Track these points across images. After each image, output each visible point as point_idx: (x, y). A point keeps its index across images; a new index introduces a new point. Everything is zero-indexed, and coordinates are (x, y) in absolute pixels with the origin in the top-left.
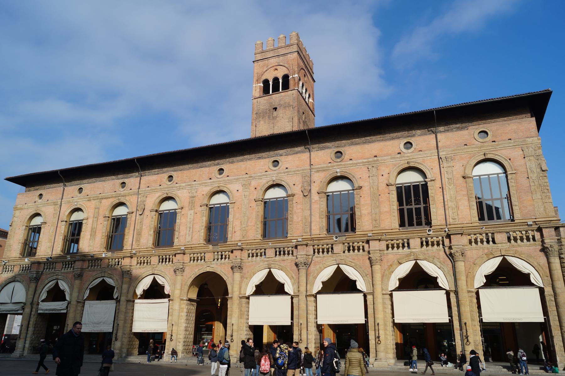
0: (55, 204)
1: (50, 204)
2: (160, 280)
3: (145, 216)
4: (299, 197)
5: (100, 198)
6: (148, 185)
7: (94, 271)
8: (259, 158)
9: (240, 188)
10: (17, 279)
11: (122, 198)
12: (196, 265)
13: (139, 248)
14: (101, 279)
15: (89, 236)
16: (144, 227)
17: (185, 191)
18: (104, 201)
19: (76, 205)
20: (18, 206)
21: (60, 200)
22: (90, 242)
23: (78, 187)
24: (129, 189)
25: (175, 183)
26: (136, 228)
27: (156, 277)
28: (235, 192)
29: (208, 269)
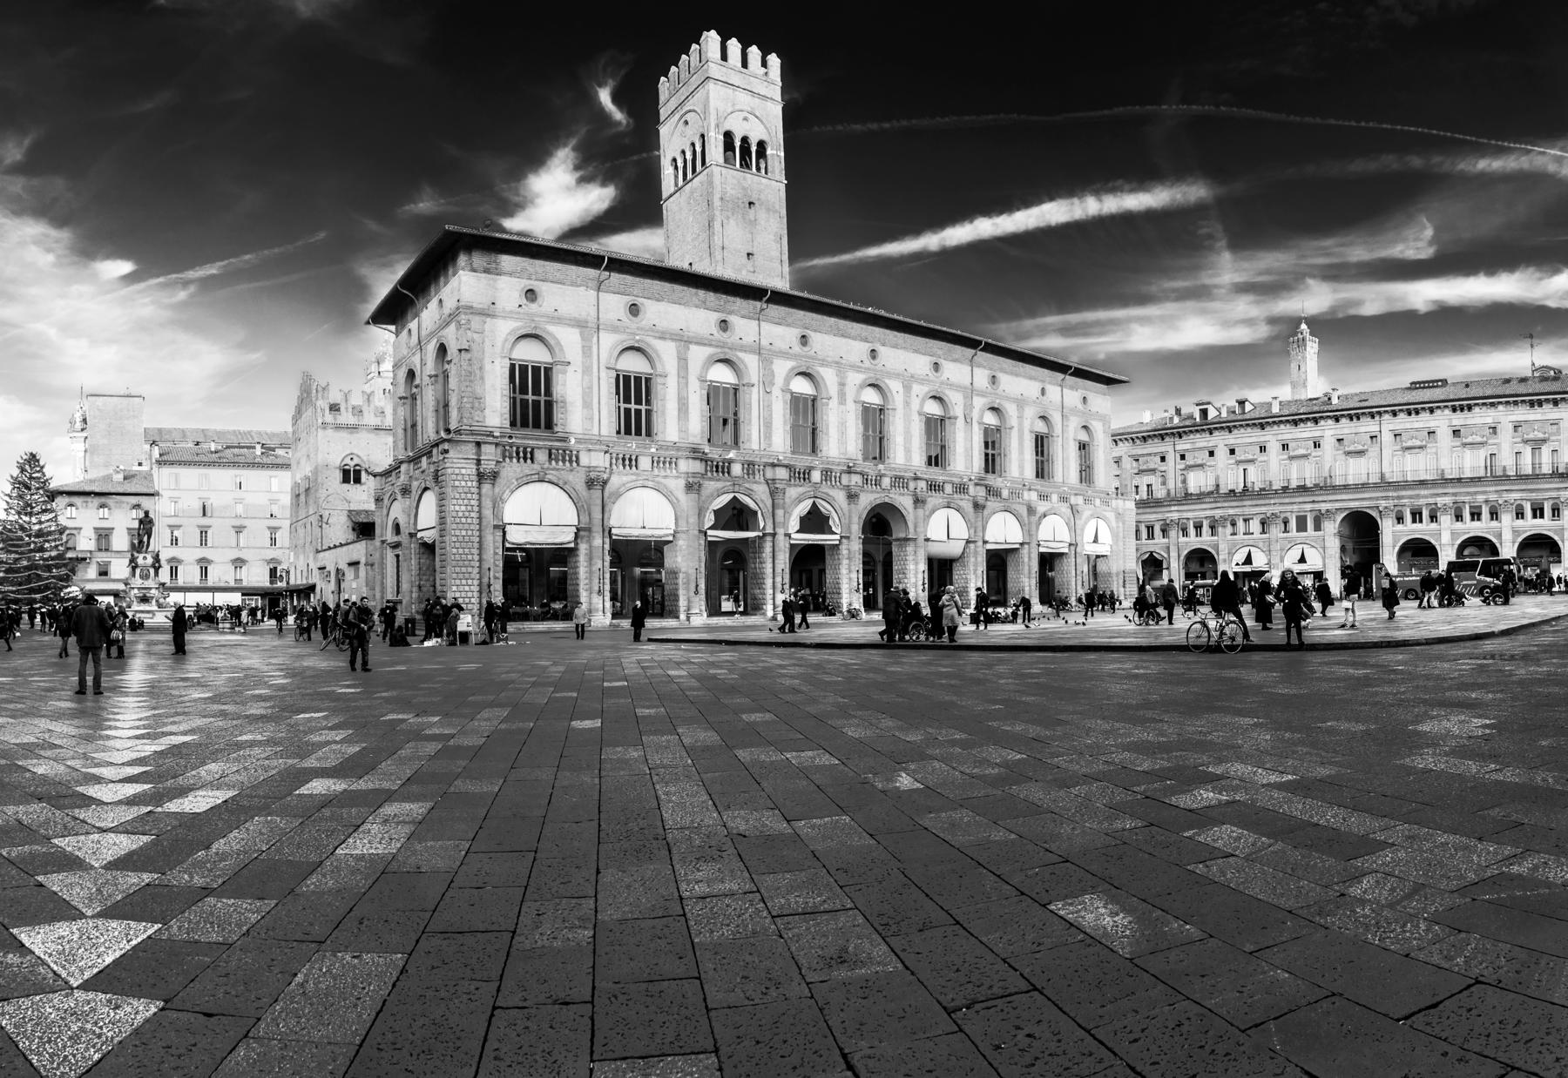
1: (568, 322)
2: (824, 507)
3: (774, 398)
4: (960, 422)
7: (718, 480)
9: (901, 390)
10: (548, 476)
12: (872, 492)
14: (731, 496)
15: (676, 413)
16: (774, 416)
17: (830, 370)
19: (638, 341)
27: (819, 501)
28: (894, 393)
29: (887, 500)
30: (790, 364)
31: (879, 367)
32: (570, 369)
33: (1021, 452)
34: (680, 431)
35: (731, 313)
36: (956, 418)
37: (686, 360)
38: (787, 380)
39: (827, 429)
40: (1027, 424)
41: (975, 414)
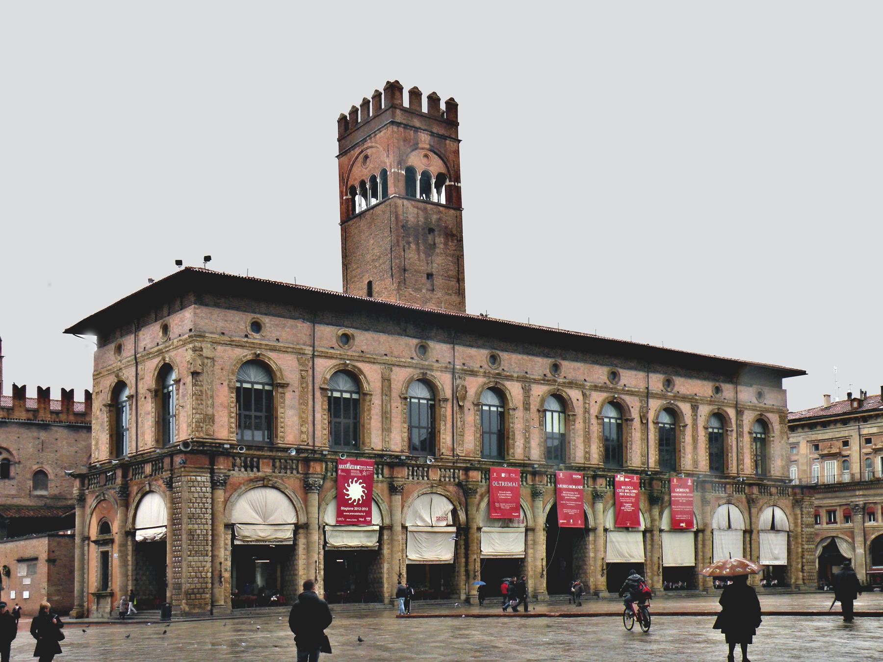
0: (300, 353)
5: (390, 363)
6: (464, 362)
8: (596, 362)
9: (581, 398)
11: (429, 372)
13: (463, 455)
18: (393, 368)
20: (207, 335)
21: (311, 348)
22: (384, 434)
23: (341, 332)
24: (434, 360)
25: (501, 369)
26: (455, 424)
28: (574, 401)
30: (481, 380)
31: (560, 380)
32: (290, 389)
33: (695, 447)
34: (383, 440)
35: (428, 338)
36: (632, 420)
37: (389, 380)
38: (479, 394)
39: (514, 435)
40: (701, 422)
41: (651, 416)
